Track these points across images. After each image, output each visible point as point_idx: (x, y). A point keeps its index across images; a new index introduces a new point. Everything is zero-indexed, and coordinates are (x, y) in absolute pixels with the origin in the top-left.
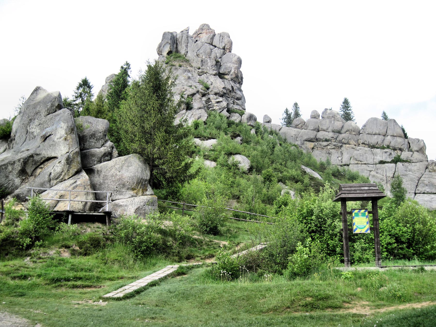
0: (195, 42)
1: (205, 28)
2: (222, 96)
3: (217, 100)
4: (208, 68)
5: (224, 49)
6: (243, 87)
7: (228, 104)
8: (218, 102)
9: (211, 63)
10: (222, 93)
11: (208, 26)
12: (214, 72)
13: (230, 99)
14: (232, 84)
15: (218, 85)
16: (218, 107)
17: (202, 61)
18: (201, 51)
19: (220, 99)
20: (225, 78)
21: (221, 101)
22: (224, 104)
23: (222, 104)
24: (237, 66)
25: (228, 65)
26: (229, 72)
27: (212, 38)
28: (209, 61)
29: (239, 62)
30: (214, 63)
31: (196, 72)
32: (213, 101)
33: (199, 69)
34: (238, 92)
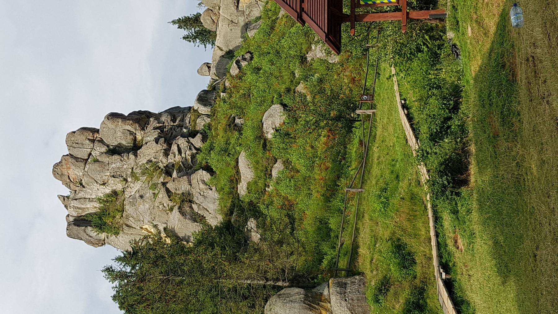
0: (84, 187)
2: (170, 145)
3: (177, 153)
4: (125, 167)
6: (155, 110)
7: (183, 136)
8: (180, 152)
9: (115, 162)
10: (165, 145)
12: (132, 156)
13: (174, 133)
14: (150, 128)
15: (152, 151)
16: (188, 152)
17: (113, 176)
18: (98, 178)
20: (142, 140)
21: (178, 146)
23: (182, 146)
24: (120, 120)
26: (131, 133)
28: (114, 165)
30: (116, 157)
31: (132, 185)
32: (178, 158)
33: (126, 180)
34: (163, 119)
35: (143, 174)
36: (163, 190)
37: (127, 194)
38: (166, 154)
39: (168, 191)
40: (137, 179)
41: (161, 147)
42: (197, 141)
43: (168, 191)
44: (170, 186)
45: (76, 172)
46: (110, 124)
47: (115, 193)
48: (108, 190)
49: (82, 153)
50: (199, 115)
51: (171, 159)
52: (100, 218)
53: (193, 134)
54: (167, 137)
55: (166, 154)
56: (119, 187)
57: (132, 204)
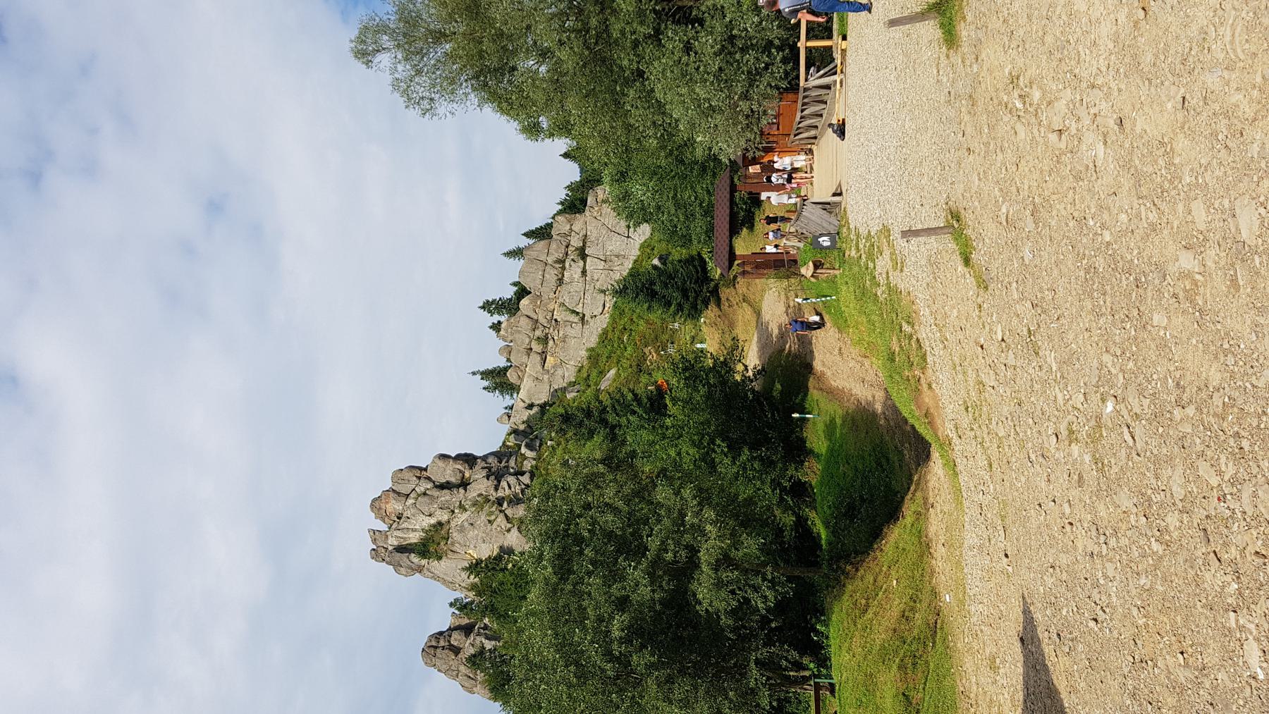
1: (376, 505)
2: (499, 482)
5: (419, 478)
6: (479, 453)
7: (511, 474)
9: (445, 496)
11: (374, 500)
14: (477, 467)
18: (425, 510)
19: (504, 484)
22: (512, 479)
25: (449, 473)
26: (460, 471)
27: (399, 494)
29: (444, 457)
30: (446, 491)
32: (507, 492)
34: (490, 460)
35: (474, 505)
36: (502, 515)
37: (453, 524)
38: (496, 489)
39: (506, 516)
40: (466, 510)
41: (491, 483)
42: (526, 479)
43: (506, 516)
44: (509, 512)
45: (394, 506)
46: (441, 463)
47: (440, 524)
48: (433, 521)
49: (405, 489)
50: (526, 458)
51: (500, 494)
52: (424, 545)
53: (522, 474)
54: (497, 476)
55: (496, 489)
56: (444, 517)
57: (462, 529)
